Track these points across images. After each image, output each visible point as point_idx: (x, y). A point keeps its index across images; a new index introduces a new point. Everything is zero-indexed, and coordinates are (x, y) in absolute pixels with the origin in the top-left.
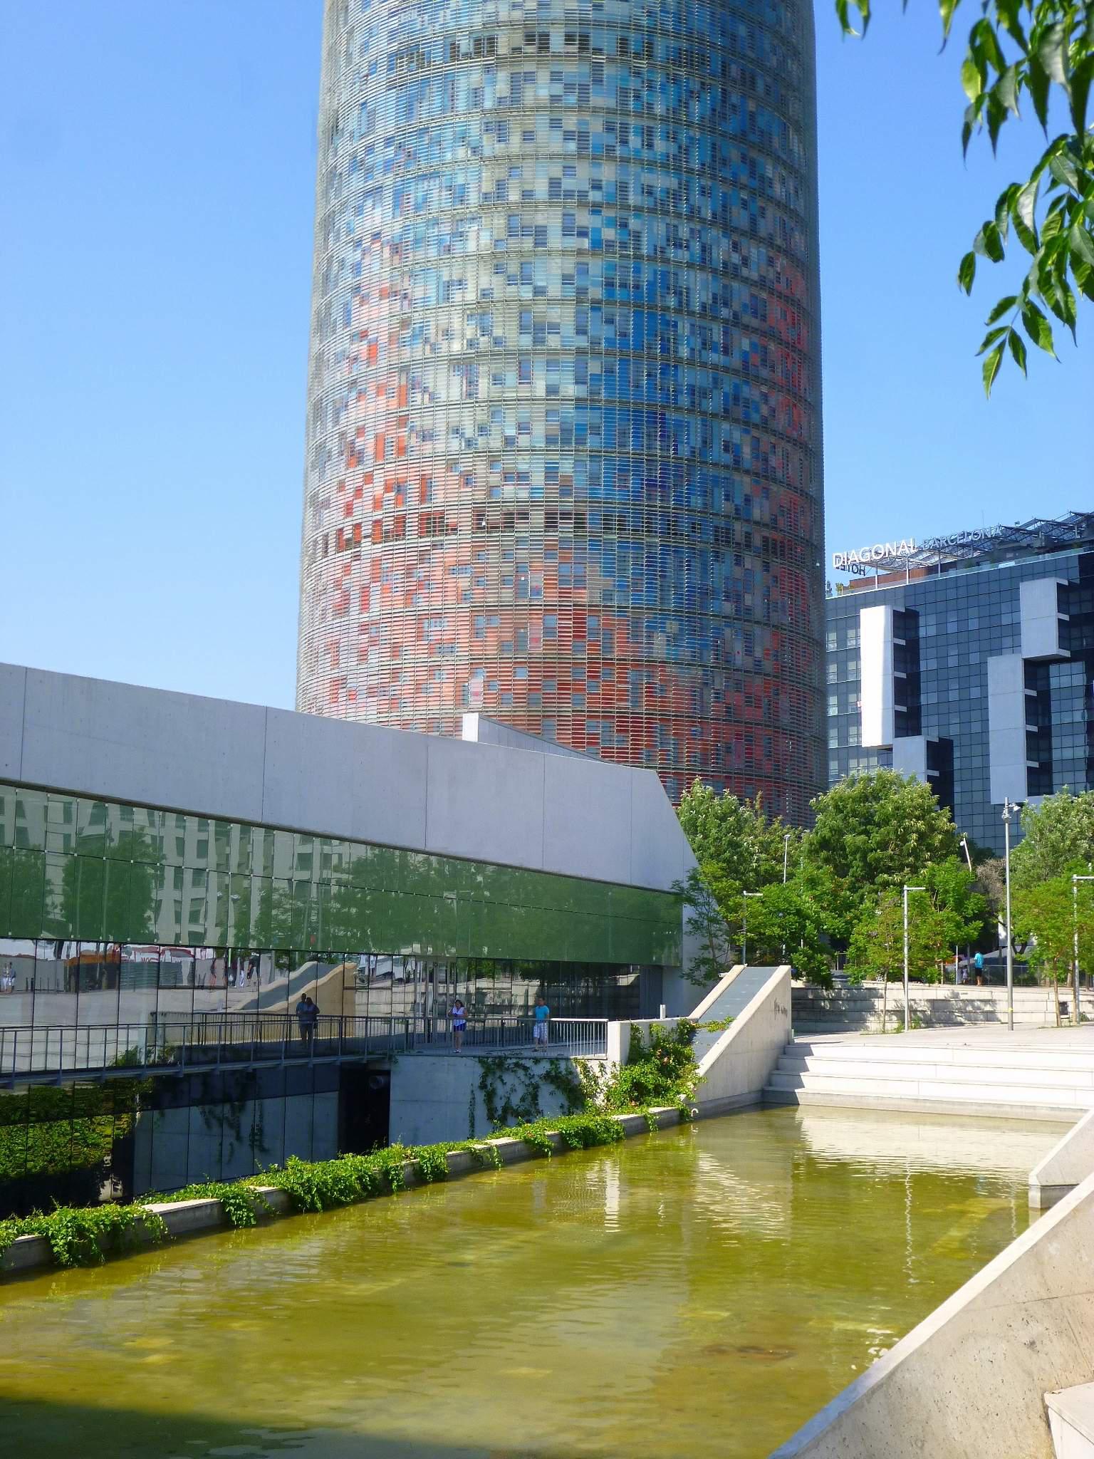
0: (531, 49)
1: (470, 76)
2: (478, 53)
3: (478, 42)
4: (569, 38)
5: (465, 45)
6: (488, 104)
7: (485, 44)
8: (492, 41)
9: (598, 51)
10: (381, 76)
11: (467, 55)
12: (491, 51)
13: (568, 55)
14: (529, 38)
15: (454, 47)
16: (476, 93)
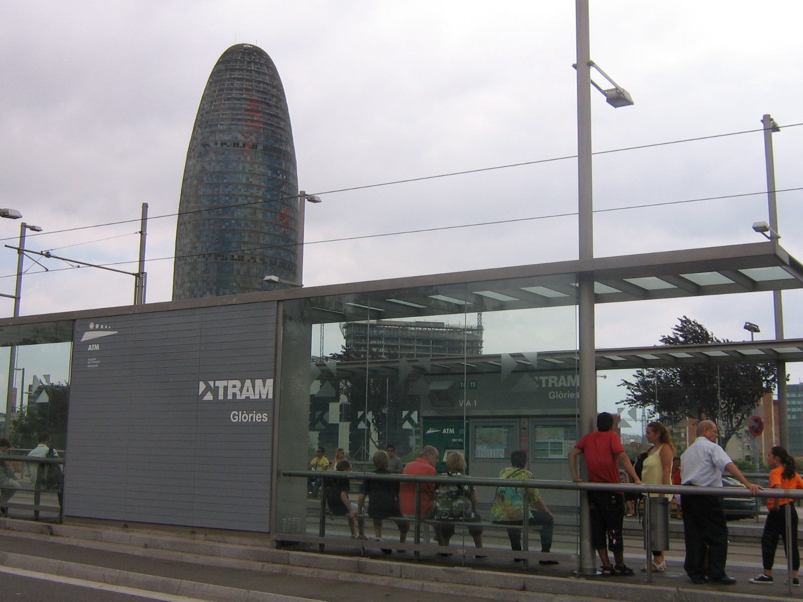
0: (252, 261)
1: (237, 266)
2: (239, 260)
3: (239, 257)
4: (261, 259)
5: (236, 257)
6: (242, 273)
7: (241, 259)
8: (243, 257)
9: (266, 263)
10: (212, 259)
11: (236, 260)
12: (242, 260)
13: (260, 263)
14: (252, 258)
15: (233, 256)
16: (239, 271)
